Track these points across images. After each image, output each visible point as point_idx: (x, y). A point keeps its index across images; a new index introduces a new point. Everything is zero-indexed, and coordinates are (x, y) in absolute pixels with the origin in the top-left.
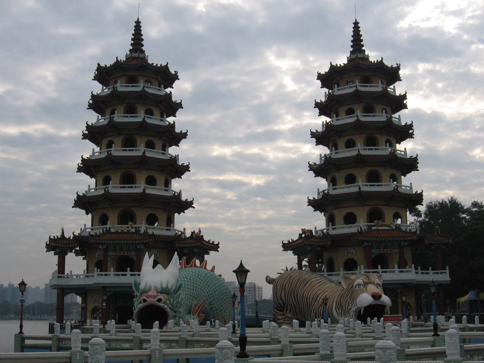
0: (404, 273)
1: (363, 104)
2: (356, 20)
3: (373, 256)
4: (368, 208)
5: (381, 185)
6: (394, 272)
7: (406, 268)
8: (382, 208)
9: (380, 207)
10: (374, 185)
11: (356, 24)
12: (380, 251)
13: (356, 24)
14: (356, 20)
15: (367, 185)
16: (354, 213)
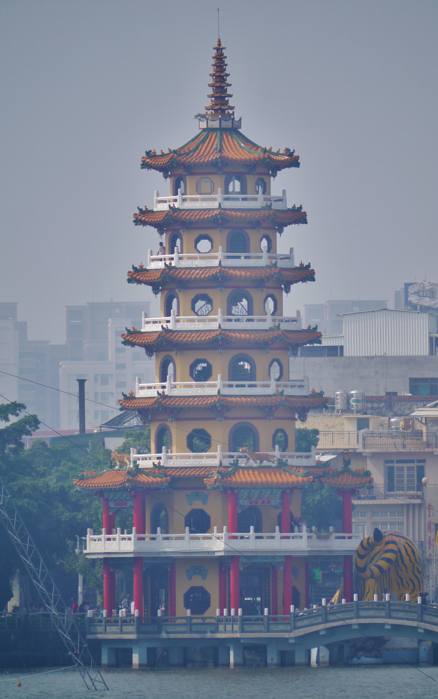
0: (291, 540)
1: (228, 231)
2: (219, 41)
3: (240, 512)
4: (232, 423)
5: (255, 386)
6: (273, 537)
7: (293, 531)
8: (254, 422)
9: (254, 422)
10: (243, 386)
11: (219, 49)
12: (251, 502)
13: (219, 49)
14: (219, 41)
15: (231, 386)
16: (209, 431)
